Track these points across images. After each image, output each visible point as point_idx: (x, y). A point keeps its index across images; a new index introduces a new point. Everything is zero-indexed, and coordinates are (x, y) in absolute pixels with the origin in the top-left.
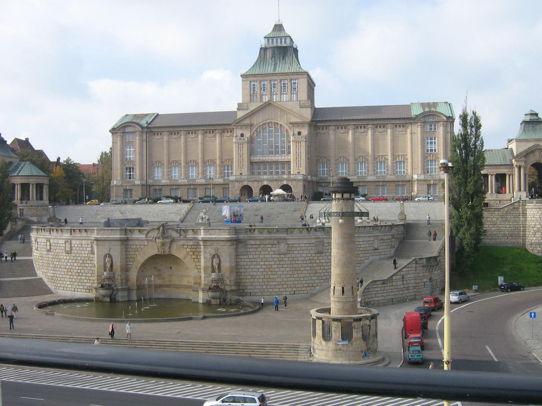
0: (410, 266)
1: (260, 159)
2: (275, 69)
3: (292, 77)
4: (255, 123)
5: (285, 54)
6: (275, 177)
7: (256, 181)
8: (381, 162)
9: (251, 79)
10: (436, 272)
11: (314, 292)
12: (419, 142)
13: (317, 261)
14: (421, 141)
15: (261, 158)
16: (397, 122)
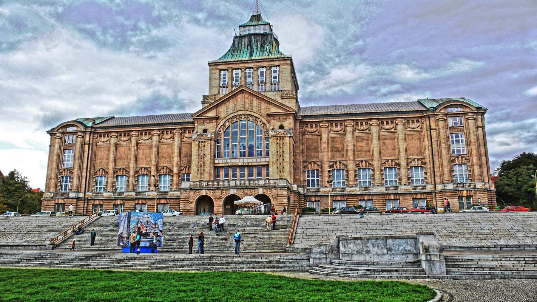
1: (227, 163)
2: (251, 55)
3: (272, 63)
4: (222, 115)
5: (264, 41)
7: (218, 188)
15: (229, 161)
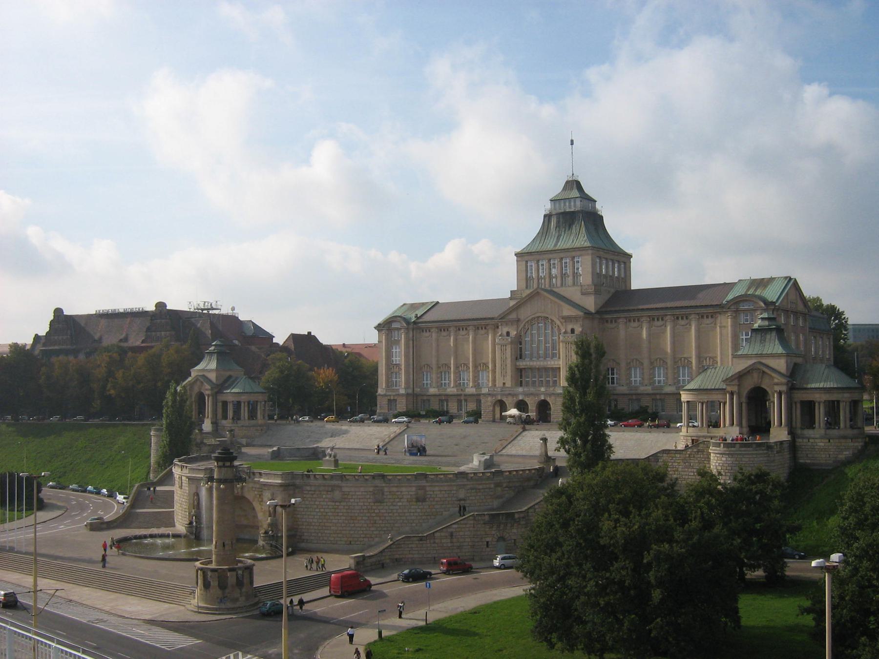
0: (465, 522)
3: (573, 254)
4: (522, 317)
6: (532, 390)
8: (684, 367)
9: (526, 258)
10: (515, 531)
11: (373, 543)
12: (730, 339)
13: (377, 511)
14: (732, 338)
16: (703, 310)
